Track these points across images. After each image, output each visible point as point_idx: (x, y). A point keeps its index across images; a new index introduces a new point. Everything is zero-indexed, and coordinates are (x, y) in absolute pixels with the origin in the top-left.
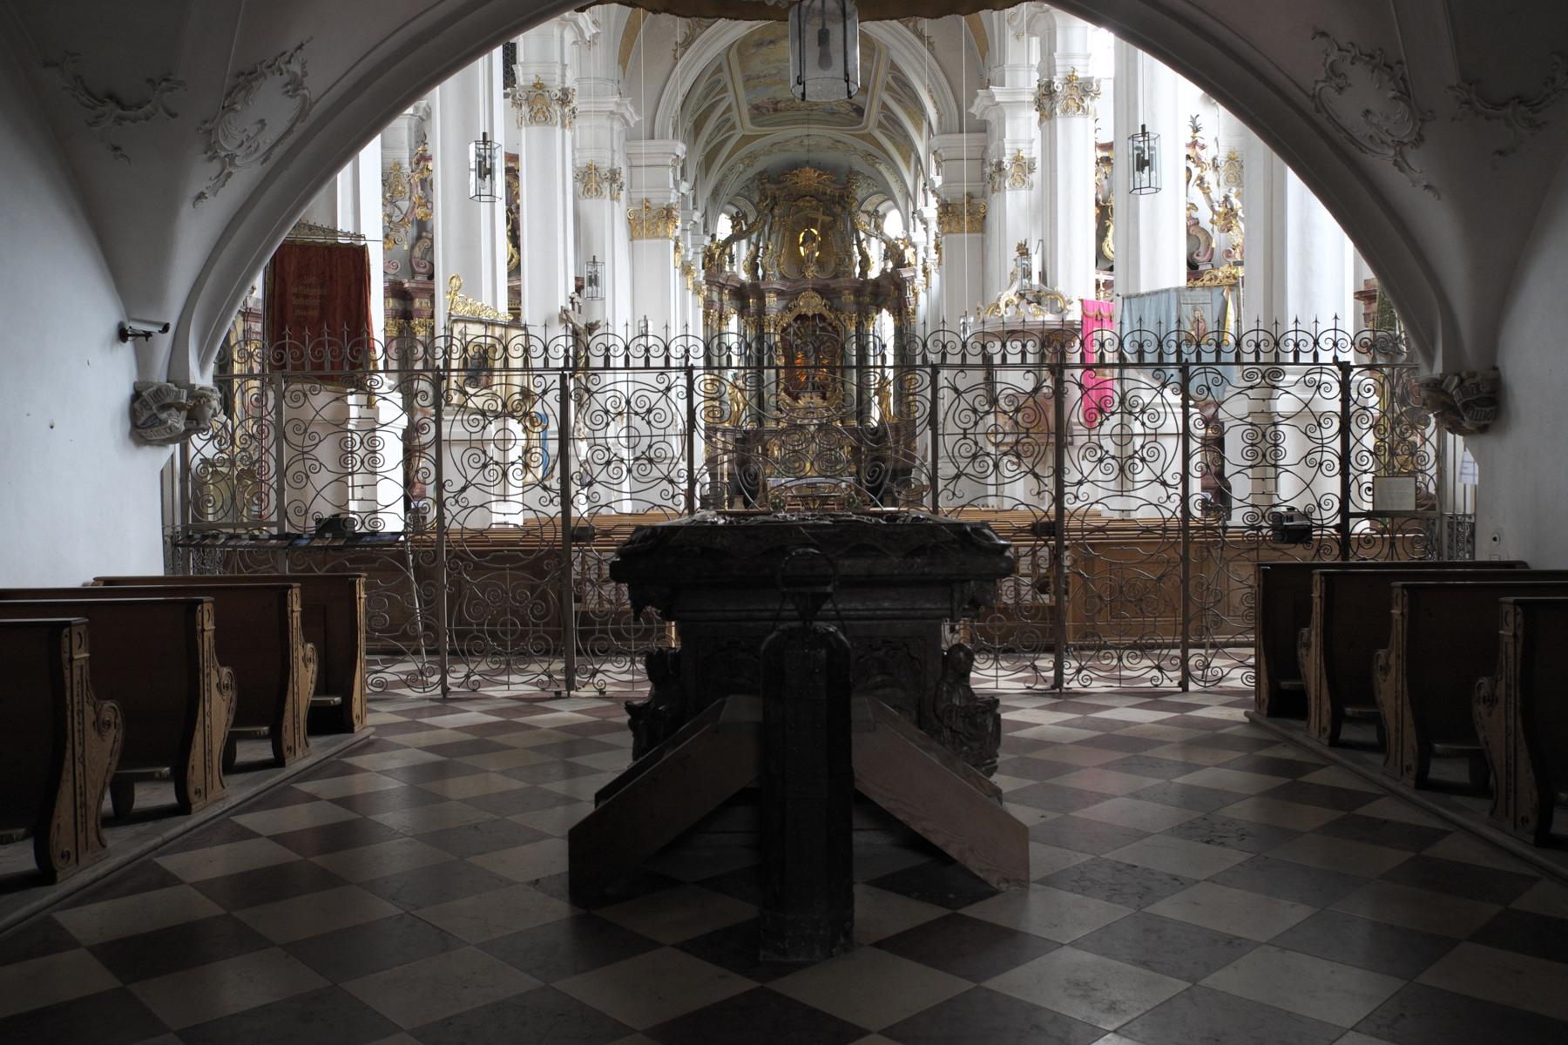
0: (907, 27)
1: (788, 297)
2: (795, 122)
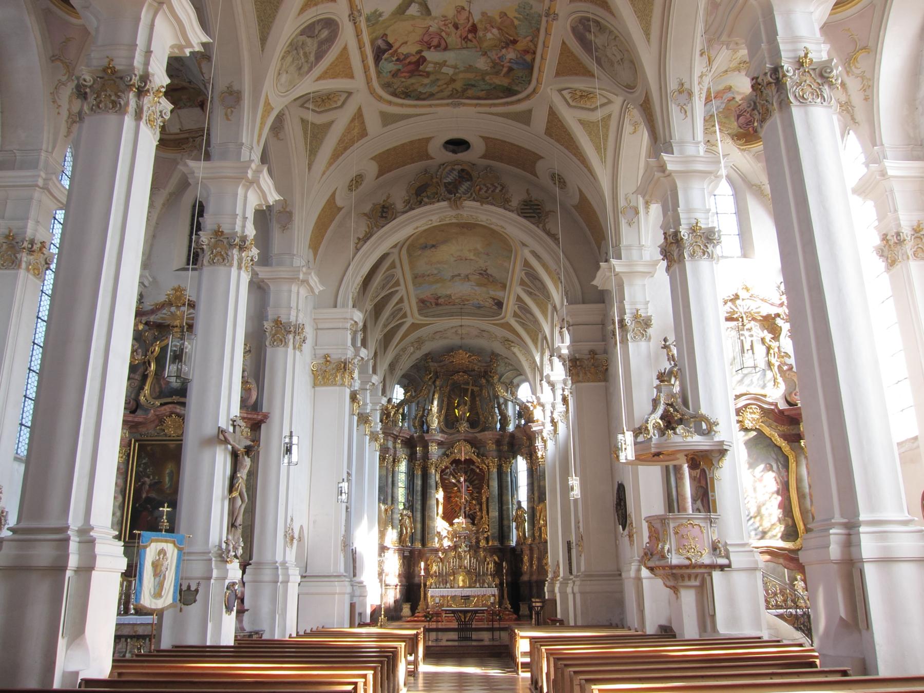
0: (538, 227)
1: (445, 446)
2: (451, 314)
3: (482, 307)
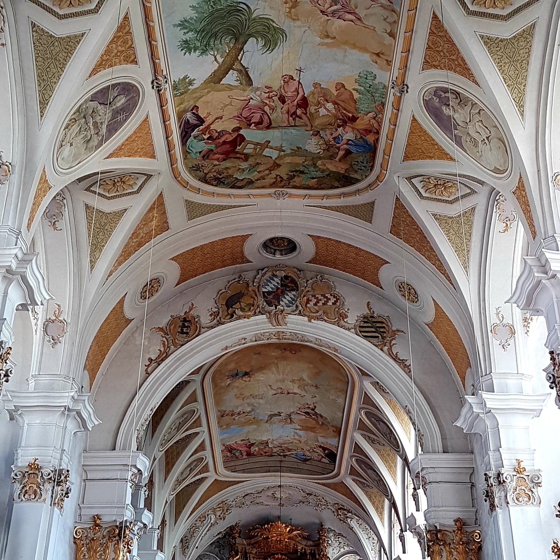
0: (382, 350)
2: (268, 470)
3: (308, 460)
